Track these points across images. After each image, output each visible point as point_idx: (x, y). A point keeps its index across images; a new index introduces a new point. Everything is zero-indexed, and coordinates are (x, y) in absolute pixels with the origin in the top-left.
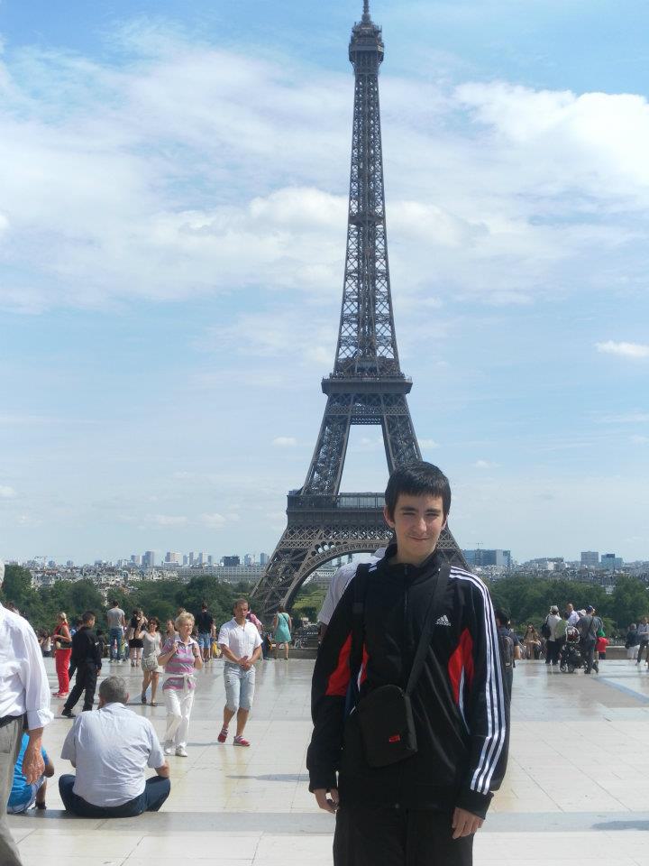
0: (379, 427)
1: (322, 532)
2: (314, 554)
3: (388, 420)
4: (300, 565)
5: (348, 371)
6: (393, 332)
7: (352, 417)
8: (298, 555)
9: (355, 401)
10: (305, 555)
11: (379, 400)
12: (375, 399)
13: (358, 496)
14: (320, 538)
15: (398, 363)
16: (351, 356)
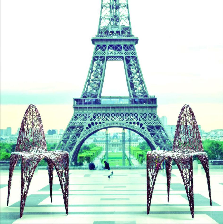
0: (123, 61)
1: (92, 117)
2: (87, 128)
3: (126, 59)
5: (105, 33)
6: (128, 12)
7: (107, 57)
8: (81, 128)
9: (109, 48)
11: (121, 48)
12: (119, 48)
13: (111, 98)
14: (91, 120)
15: (131, 29)
16: (107, 25)
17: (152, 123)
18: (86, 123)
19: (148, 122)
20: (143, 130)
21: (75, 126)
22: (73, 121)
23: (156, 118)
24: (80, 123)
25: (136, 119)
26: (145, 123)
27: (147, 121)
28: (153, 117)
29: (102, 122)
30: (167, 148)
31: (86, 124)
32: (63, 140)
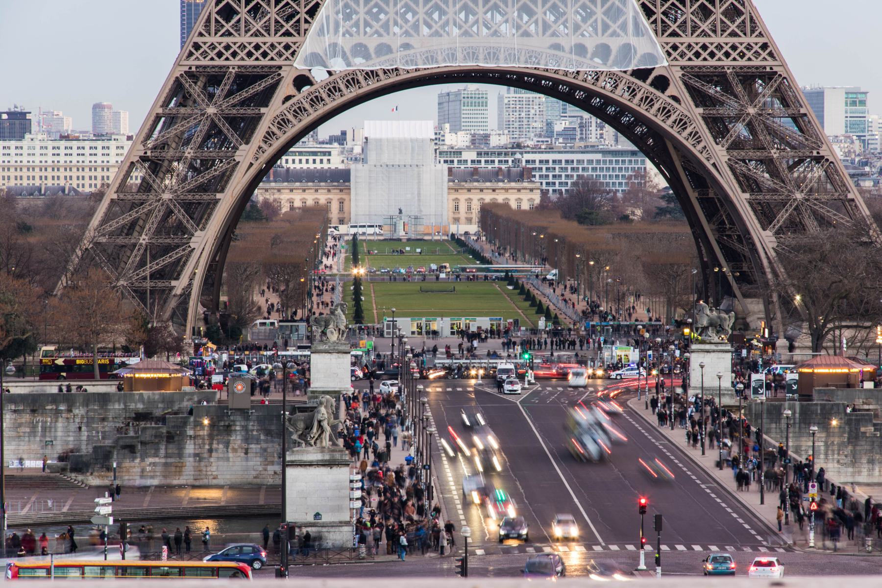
4: (256, 120)
10: (270, 91)
17: (719, 54)
18: (294, 47)
19: (689, 46)
20: (658, 93)
21: (221, 67)
22: (209, 39)
23: (739, 21)
24: (257, 47)
25: (614, 27)
26: (669, 54)
27: (686, 39)
28: (725, 13)
29: (394, 47)
30: (815, 213)
31: (293, 54)
32: (144, 159)
